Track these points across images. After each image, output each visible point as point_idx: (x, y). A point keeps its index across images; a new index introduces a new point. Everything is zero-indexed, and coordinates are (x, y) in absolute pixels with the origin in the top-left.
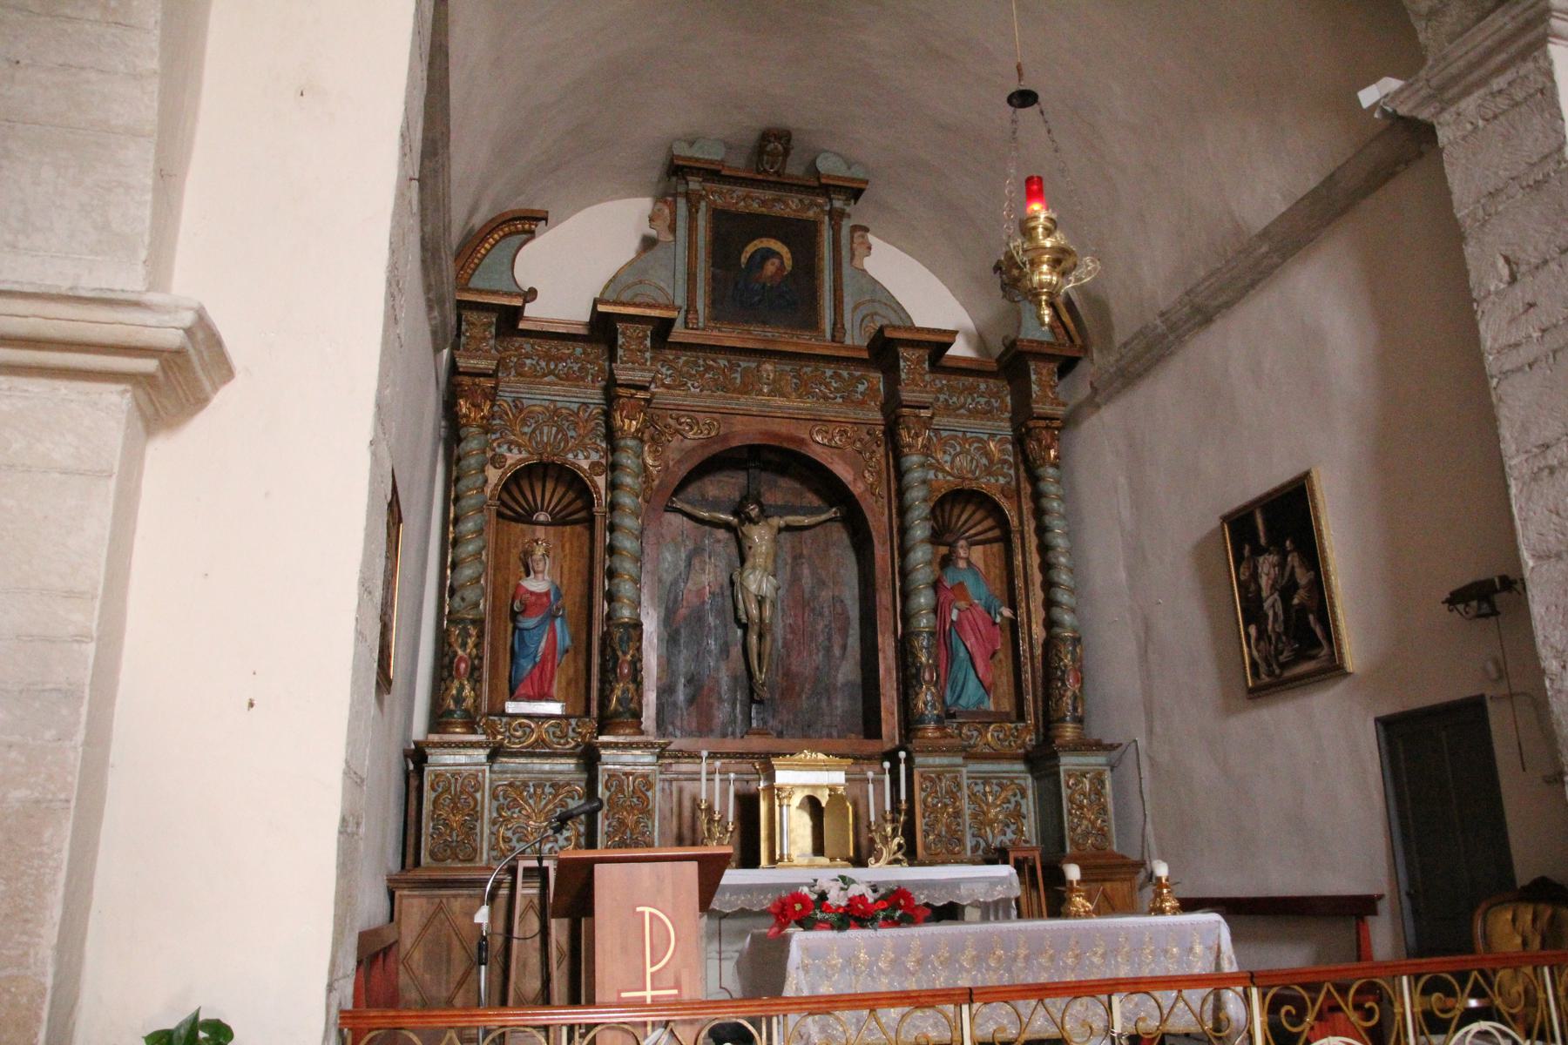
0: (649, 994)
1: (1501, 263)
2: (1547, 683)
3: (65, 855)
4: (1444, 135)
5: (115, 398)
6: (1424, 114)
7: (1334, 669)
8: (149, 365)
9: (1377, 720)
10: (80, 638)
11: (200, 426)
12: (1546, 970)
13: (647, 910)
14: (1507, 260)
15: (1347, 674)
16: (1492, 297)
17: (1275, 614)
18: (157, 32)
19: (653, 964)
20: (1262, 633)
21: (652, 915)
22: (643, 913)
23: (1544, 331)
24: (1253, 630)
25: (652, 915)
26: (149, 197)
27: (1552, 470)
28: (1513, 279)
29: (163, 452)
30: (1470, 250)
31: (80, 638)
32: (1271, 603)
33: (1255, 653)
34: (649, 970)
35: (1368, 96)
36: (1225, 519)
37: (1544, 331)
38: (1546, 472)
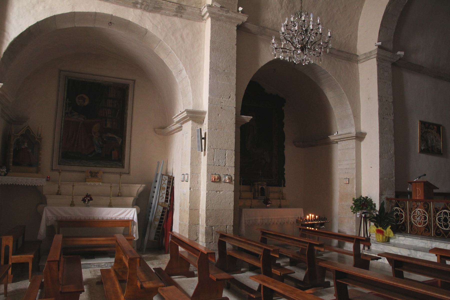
0: (418, 198)
3: (355, 182)
5: (354, 141)
8: (355, 138)
10: (354, 163)
11: (365, 140)
13: (418, 188)
18: (349, 105)
19: (418, 195)
21: (418, 189)
22: (417, 189)
25: (418, 189)
26: (353, 120)
29: (363, 143)
31: (354, 163)
34: (418, 195)
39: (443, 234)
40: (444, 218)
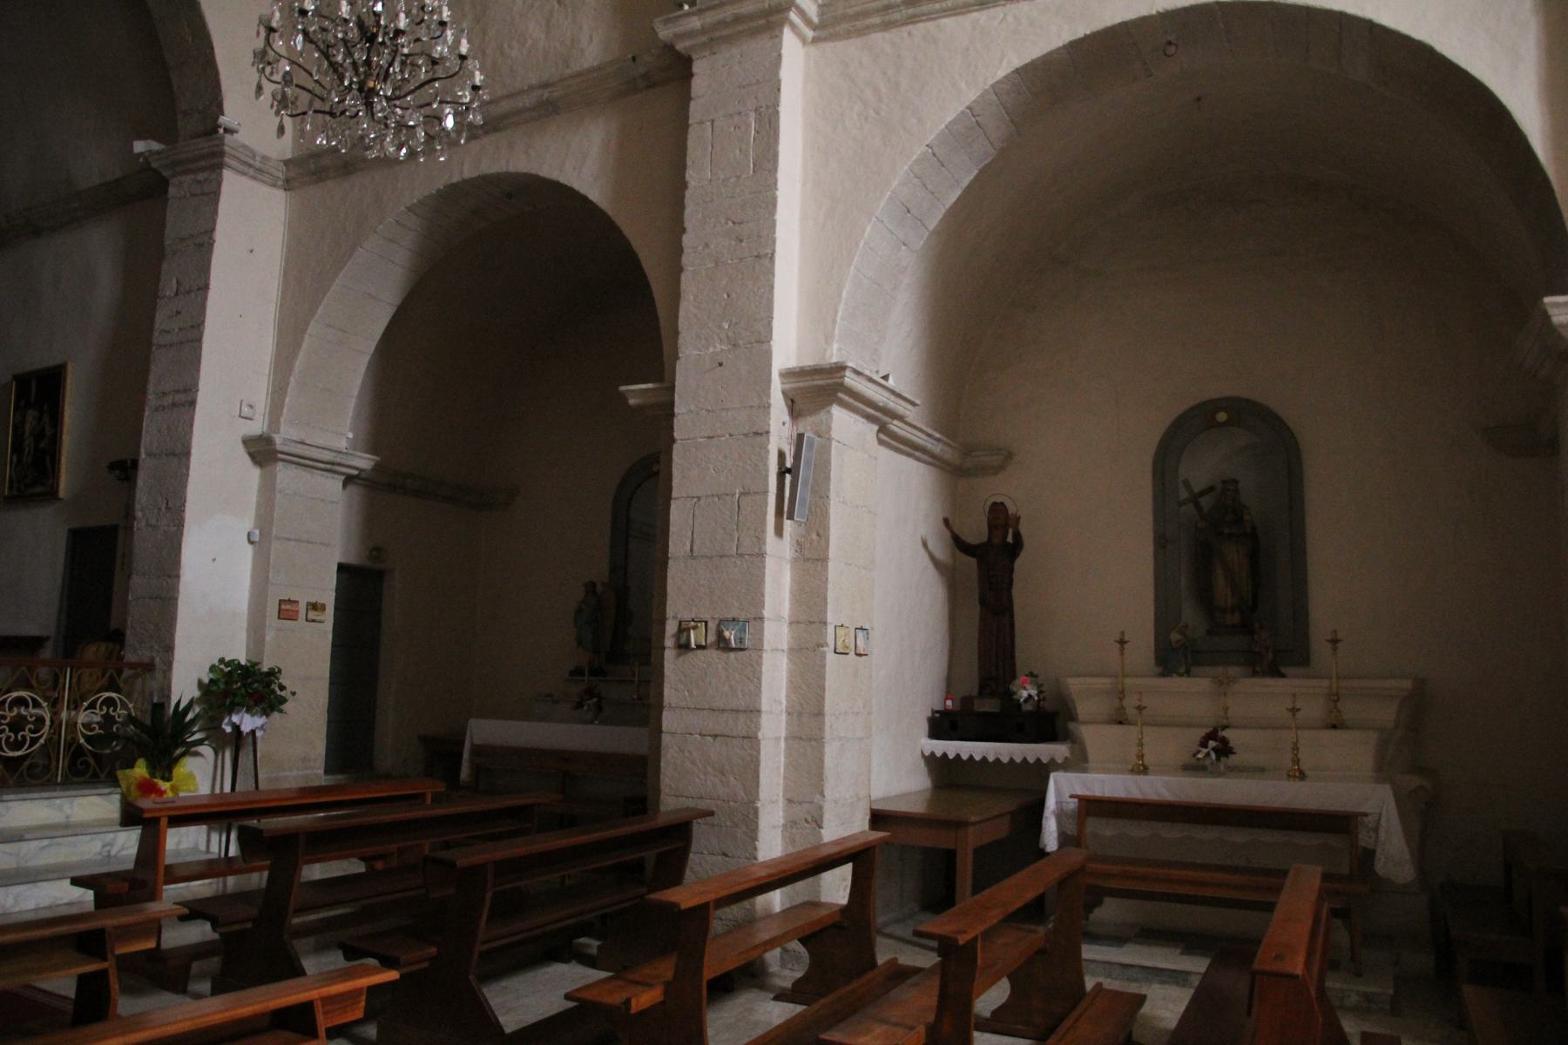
1: (174, 281)
2: (135, 523)
4: (172, 191)
6: (166, 173)
7: (52, 495)
9: (70, 531)
12: (69, 670)
14: (178, 282)
15: (59, 499)
16: (166, 299)
17: (29, 451)
20: (19, 461)
23: (181, 329)
24: (15, 458)
27: (164, 408)
28: (177, 294)
30: (165, 266)
32: (29, 442)
33: (13, 474)
35: (139, 146)
36: (15, 377)
37: (181, 329)
38: (161, 408)
39: (94, 770)
40: (114, 716)
